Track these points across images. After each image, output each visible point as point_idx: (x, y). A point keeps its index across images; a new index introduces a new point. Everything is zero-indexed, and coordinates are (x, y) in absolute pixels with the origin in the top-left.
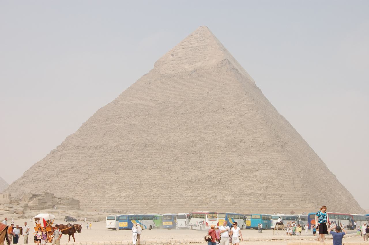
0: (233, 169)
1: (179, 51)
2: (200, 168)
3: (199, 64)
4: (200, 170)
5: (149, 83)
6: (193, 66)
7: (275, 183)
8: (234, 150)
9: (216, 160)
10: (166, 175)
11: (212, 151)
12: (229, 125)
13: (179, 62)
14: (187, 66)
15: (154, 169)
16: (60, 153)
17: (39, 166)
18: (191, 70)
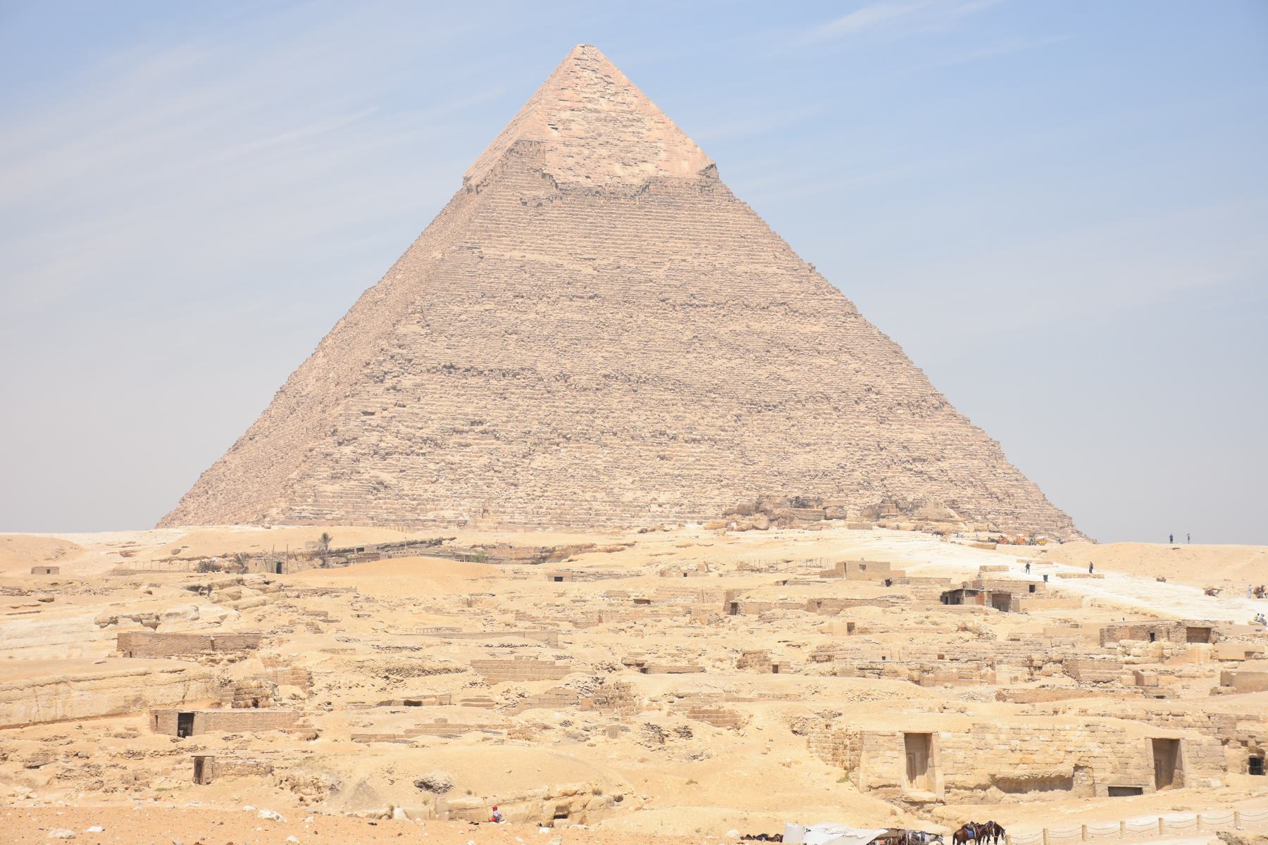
0: (883, 452)
1: (566, 115)
2: (808, 445)
3: (650, 169)
4: (808, 449)
5: (534, 204)
6: (636, 170)
7: (995, 490)
8: (862, 407)
9: (835, 429)
10: (732, 457)
11: (810, 406)
12: (820, 348)
13: (586, 152)
14: (618, 169)
15: (694, 440)
16: (407, 382)
17: (365, 413)
18: (637, 182)
